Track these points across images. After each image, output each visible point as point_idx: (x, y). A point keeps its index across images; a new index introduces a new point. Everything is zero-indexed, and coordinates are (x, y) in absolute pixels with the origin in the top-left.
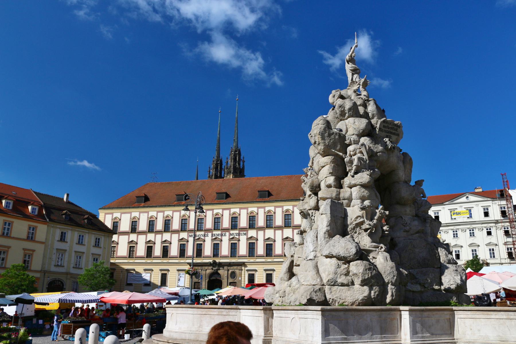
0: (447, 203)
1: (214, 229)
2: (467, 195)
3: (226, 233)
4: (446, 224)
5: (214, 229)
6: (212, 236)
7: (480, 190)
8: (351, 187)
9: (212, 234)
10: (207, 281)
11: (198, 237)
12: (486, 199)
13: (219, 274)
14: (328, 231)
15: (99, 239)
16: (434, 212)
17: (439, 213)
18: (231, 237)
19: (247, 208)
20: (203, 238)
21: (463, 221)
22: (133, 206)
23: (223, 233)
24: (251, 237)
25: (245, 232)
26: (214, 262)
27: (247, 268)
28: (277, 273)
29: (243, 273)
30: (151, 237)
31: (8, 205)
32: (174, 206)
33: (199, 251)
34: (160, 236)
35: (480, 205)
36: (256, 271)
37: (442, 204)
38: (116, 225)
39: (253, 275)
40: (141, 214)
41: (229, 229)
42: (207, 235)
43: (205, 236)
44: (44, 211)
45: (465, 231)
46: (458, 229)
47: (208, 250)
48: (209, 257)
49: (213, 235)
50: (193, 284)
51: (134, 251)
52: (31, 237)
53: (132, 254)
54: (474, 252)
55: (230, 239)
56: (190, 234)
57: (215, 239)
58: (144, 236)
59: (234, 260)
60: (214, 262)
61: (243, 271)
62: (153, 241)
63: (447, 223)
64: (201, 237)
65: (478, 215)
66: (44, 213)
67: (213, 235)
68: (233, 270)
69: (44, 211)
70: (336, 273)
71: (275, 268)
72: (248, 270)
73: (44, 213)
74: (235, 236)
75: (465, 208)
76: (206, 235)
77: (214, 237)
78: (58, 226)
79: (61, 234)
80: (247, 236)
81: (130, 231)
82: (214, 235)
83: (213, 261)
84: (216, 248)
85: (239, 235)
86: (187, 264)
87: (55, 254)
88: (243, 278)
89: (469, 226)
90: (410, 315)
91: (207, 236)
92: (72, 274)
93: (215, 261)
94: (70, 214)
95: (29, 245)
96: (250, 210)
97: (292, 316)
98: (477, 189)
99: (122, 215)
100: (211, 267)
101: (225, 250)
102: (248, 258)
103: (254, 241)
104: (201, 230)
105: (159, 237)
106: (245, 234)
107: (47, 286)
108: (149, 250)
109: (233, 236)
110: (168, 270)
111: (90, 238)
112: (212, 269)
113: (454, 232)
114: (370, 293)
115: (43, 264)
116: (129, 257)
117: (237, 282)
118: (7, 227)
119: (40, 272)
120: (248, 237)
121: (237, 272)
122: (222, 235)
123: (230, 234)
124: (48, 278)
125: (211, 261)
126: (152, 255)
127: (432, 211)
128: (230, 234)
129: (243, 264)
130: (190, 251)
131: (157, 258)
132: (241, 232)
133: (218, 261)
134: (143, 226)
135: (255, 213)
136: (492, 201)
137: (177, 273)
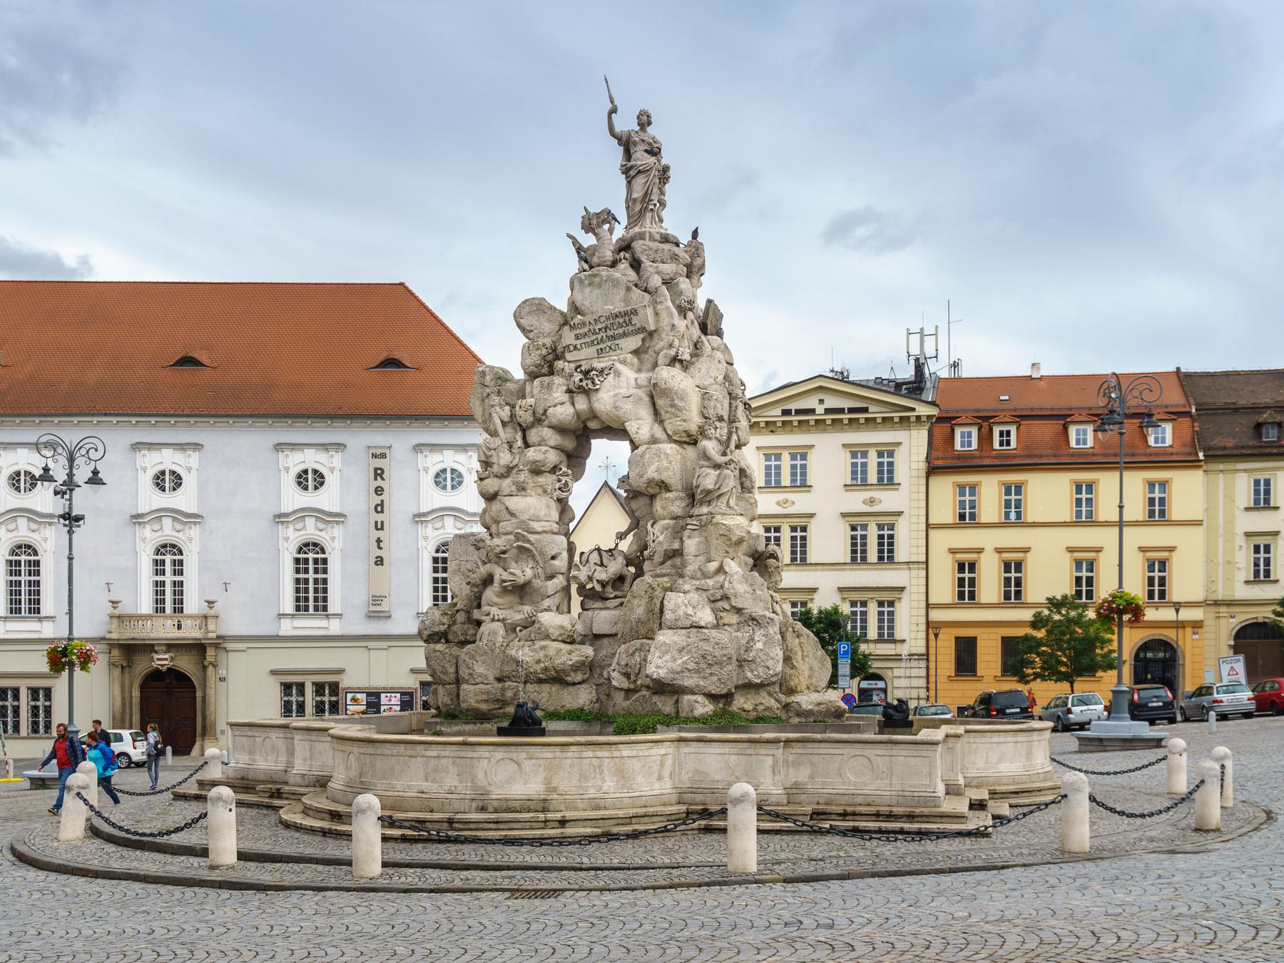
52: (1157, 512)
87: (1244, 548)
95: (1157, 536)
107: (1232, 643)
115: (1211, 582)
118: (1084, 496)
124: (1231, 620)
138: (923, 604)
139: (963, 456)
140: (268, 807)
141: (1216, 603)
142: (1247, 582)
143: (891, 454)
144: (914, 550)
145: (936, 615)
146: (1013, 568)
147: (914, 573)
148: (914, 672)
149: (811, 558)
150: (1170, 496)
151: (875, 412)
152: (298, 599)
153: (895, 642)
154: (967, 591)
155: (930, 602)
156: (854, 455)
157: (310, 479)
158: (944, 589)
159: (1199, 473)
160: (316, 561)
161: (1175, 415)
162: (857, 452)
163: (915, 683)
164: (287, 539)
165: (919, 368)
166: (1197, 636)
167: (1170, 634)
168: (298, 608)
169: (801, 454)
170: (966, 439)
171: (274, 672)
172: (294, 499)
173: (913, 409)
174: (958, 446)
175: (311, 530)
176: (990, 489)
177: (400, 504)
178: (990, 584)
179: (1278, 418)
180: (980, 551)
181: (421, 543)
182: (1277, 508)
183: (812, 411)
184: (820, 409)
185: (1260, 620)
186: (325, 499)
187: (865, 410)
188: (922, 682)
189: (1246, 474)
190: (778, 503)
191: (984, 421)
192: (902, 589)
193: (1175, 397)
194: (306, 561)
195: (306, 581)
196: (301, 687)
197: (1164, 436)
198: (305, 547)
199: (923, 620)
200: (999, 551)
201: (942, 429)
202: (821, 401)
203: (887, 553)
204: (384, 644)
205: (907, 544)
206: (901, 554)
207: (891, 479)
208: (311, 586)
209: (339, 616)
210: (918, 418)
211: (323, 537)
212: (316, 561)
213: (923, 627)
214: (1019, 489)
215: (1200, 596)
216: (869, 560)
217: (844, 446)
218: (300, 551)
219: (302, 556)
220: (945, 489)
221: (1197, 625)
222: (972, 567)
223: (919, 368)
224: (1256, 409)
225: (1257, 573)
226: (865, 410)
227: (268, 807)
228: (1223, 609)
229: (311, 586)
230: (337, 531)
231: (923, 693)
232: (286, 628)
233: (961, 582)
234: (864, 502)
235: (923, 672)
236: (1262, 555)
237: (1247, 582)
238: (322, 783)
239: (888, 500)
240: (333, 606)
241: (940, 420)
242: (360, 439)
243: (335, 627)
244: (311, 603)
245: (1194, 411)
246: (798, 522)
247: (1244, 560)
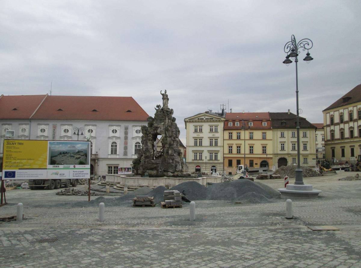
22: (341, 105)
30: (351, 124)
40: (344, 110)
52: (264, 138)
81: (340, 122)
95: (264, 142)
108: (352, 132)
115: (273, 151)
119: (273, 154)
131: (356, 137)
134: (346, 118)
138: (223, 154)
139: (229, 127)
140: (112, 186)
141: (275, 154)
142: (280, 150)
143: (217, 127)
144: (221, 144)
145: (225, 156)
146: (239, 147)
147: (221, 148)
148: (221, 166)
149: (203, 145)
151: (214, 119)
152: (112, 152)
153: (217, 160)
154: (230, 151)
155: (224, 153)
156: (210, 127)
157: (115, 131)
158: (226, 151)
159: (272, 131)
160: (139, 146)
161: (267, 121)
162: (211, 126)
163: (221, 168)
164: (110, 141)
165: (223, 110)
167: (266, 160)
168: (111, 153)
169: (201, 126)
170: (230, 124)
171: (107, 165)
172: (111, 134)
173: (221, 119)
174: (229, 126)
175: (114, 140)
176: (235, 134)
177: (130, 136)
178: (235, 150)
179: (285, 122)
180: (233, 144)
181: (133, 143)
182: (285, 137)
183: (203, 119)
184: (205, 119)
186: (117, 135)
187: (212, 119)
188: (223, 168)
190: (197, 135)
191: (234, 121)
192: (219, 151)
193: (268, 117)
194: (137, 145)
195: (113, 149)
196: (111, 167)
197: (265, 124)
198: (113, 143)
199: (223, 156)
200: (236, 144)
201: (226, 122)
202: (205, 117)
203: (216, 144)
204: (126, 160)
205: (220, 143)
206: (219, 144)
207: (217, 131)
208: (114, 150)
209: (119, 155)
210: (222, 120)
211: (116, 141)
212: (139, 146)
213: (223, 158)
214: (240, 133)
215: (272, 153)
216: (213, 146)
217: (209, 125)
218: (112, 143)
219: (112, 144)
220: (227, 133)
221: (271, 158)
222: (231, 147)
223: (223, 110)
224: (281, 120)
225: (282, 149)
226: (212, 119)
227: (112, 186)
228: (276, 155)
229: (114, 150)
230: (119, 140)
231: (223, 170)
232: (109, 157)
233: (229, 150)
234: (212, 135)
235: (223, 166)
236: (283, 146)
237: (280, 150)
238: (119, 183)
239: (217, 135)
240: (118, 153)
241: (226, 121)
242: (123, 125)
243: (118, 157)
244: (114, 153)
245: (271, 119)
246: (201, 139)
247: (279, 146)
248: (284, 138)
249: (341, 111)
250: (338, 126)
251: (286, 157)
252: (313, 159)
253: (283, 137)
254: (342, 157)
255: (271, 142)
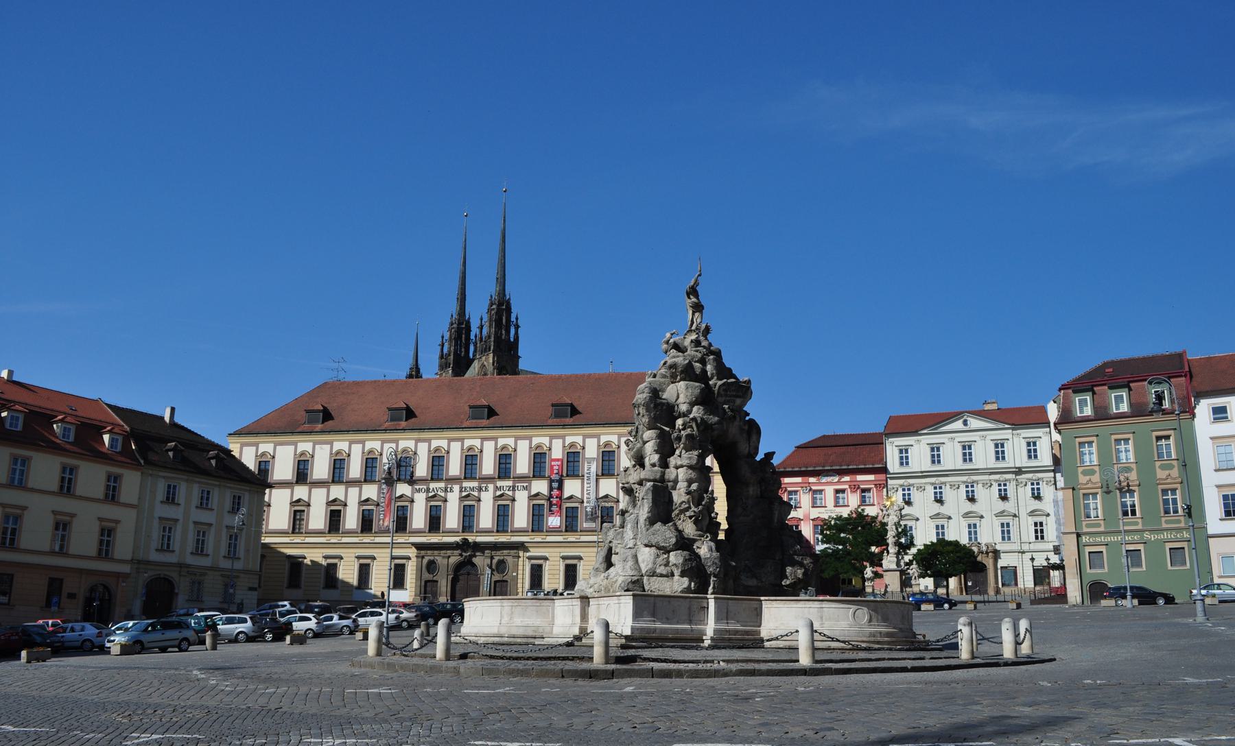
0: (925, 431)
1: (465, 478)
2: (965, 417)
3: (489, 485)
4: (922, 472)
5: (465, 478)
6: (461, 491)
7: (994, 407)
8: (677, 468)
9: (461, 488)
10: (450, 577)
11: (433, 493)
12: (1001, 426)
13: (474, 565)
14: (648, 518)
15: (239, 497)
16: (900, 448)
17: (909, 450)
18: (498, 493)
19: (530, 438)
20: (443, 494)
21: (953, 468)
22: (299, 430)
23: (482, 485)
24: (537, 495)
25: (525, 485)
26: (465, 541)
27: (528, 554)
28: (587, 563)
29: (520, 563)
30: (337, 491)
31: (67, 433)
32: (385, 430)
33: (435, 522)
34: (357, 489)
35: (989, 438)
36: (546, 559)
37: (914, 432)
38: (265, 466)
39: (540, 566)
40: (317, 447)
41: (494, 478)
42: (451, 489)
43: (446, 490)
44: (133, 444)
45: (958, 488)
46: (945, 483)
47: (452, 519)
48: (454, 532)
49: (463, 489)
50: (423, 583)
51: (303, 519)
52: (111, 495)
53: (300, 525)
54: (972, 530)
55: (496, 498)
56: (417, 487)
57: (468, 496)
58: (324, 491)
59: (503, 538)
60: (465, 541)
61: (521, 559)
62: (342, 502)
63: (923, 470)
64: (439, 493)
65: (984, 456)
66: (134, 448)
67: (463, 489)
68: (502, 558)
69: (133, 444)
70: (654, 563)
71: (582, 555)
72: (530, 558)
73: (134, 448)
74: (507, 492)
75: (959, 442)
76: (449, 490)
77: (464, 494)
78: (161, 474)
79: (168, 488)
80: (530, 492)
81: (295, 479)
82: (465, 489)
83: (463, 539)
84: (468, 515)
85: (514, 490)
86: (410, 545)
88: (520, 572)
89: (964, 478)
90: (715, 602)
91: (451, 490)
92: (188, 566)
93: (467, 539)
94: (183, 448)
95: (109, 511)
96: (536, 441)
97: (607, 603)
98: (989, 403)
99: (278, 447)
100: (459, 552)
101: (486, 518)
102: (530, 533)
103: (543, 501)
104: (439, 480)
105: (353, 492)
106: (525, 488)
108: (335, 519)
109: (503, 492)
110: (374, 558)
111: (221, 496)
112: (461, 555)
113: (935, 488)
114: (690, 584)
116: (293, 532)
117: (509, 581)
119: (132, 561)
120: (532, 494)
121: (510, 560)
122: (480, 489)
123: (497, 488)
124: (145, 575)
125: (458, 539)
126: (339, 528)
127: (896, 446)
128: (497, 487)
129: (522, 546)
130: (418, 518)
131: (350, 533)
132: (517, 485)
133: (471, 539)
134: (320, 469)
135: (545, 448)
136: (1013, 429)
137: (561, 562)
141: (139, 562)
150: (120, 486)
166: (125, 584)
185: (162, 576)
189: (163, 480)
248: (173, 507)
249: (305, 446)
250: (287, 492)
251: (174, 575)
252: (251, 589)
253: (173, 502)
254: (323, 588)
255: (133, 513)
